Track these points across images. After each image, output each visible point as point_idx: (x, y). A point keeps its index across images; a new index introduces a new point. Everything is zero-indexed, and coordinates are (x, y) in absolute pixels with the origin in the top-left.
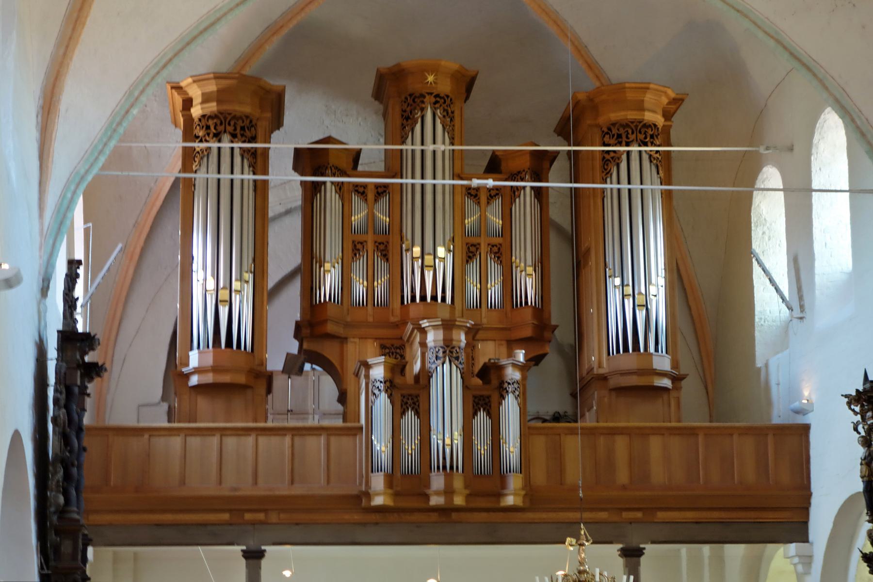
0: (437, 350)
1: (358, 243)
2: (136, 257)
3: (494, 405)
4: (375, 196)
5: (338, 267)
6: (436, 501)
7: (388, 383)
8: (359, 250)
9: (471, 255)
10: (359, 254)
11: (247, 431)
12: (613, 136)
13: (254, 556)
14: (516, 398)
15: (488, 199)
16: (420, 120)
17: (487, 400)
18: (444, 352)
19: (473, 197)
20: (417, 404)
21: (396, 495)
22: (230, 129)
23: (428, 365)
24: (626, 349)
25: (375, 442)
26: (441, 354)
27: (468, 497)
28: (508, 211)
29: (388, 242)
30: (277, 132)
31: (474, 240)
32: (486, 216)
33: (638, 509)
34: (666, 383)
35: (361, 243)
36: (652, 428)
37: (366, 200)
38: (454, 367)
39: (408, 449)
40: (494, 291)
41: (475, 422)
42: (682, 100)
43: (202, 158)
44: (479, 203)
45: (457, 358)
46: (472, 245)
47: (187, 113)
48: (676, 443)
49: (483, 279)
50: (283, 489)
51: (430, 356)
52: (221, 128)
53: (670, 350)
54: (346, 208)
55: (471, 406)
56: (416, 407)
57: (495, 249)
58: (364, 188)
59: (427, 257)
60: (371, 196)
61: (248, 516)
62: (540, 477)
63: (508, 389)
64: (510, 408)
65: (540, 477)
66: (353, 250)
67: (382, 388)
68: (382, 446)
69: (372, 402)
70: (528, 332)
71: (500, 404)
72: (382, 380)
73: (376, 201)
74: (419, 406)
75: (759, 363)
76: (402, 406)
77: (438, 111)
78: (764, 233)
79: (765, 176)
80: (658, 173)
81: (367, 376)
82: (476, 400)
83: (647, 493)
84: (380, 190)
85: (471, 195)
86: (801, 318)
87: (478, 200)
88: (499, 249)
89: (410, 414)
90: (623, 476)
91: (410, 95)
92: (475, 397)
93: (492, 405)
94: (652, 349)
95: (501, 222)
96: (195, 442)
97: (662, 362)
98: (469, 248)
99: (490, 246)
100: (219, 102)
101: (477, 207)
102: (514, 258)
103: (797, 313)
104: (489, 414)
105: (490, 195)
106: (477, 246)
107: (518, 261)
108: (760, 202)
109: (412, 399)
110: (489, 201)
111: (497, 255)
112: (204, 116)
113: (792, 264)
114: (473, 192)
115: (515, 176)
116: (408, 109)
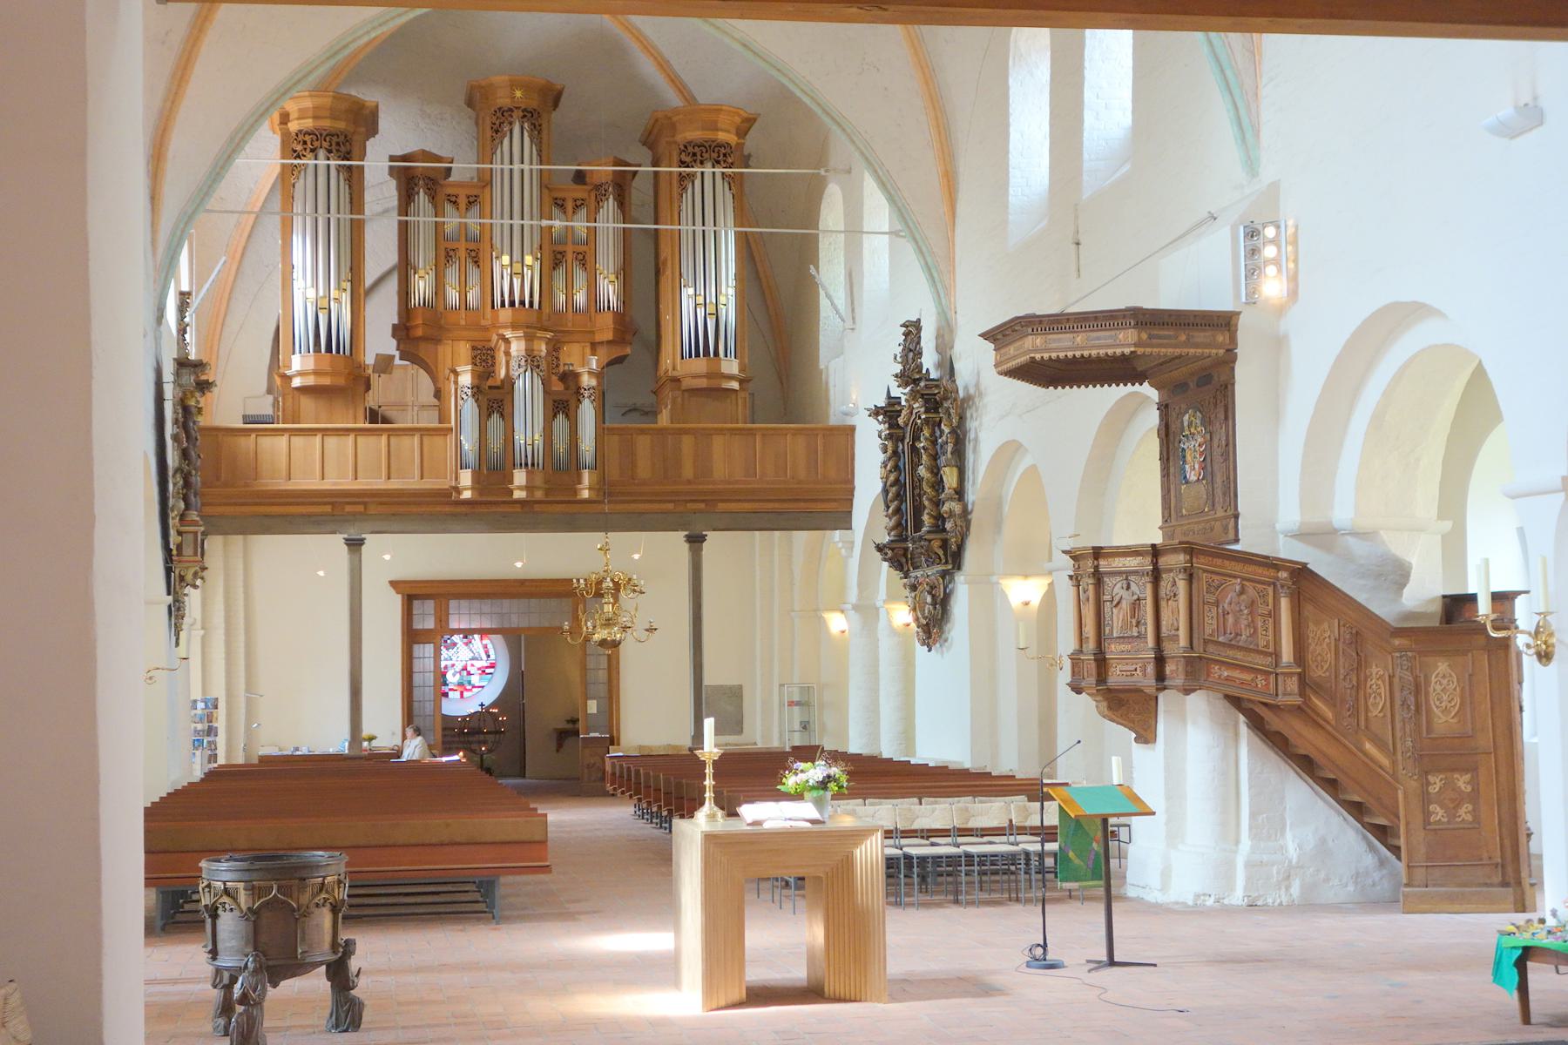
2: (238, 256)
3: (572, 407)
5: (432, 274)
6: (519, 494)
9: (558, 262)
11: (347, 431)
12: (689, 154)
13: (355, 545)
18: (526, 361)
22: (325, 144)
23: (511, 372)
24: (698, 355)
25: (464, 442)
26: (523, 363)
27: (548, 492)
30: (372, 139)
31: (560, 248)
33: (703, 501)
34: (735, 385)
36: (716, 429)
38: (535, 375)
40: (580, 298)
41: (554, 424)
42: (755, 120)
43: (299, 172)
45: (538, 367)
47: (284, 126)
50: (380, 484)
51: (514, 364)
52: (317, 144)
53: (738, 355)
57: (581, 257)
59: (514, 265)
60: (463, 205)
61: (348, 508)
62: (613, 472)
64: (587, 412)
65: (613, 472)
67: (469, 394)
68: (469, 443)
70: (609, 336)
71: (577, 407)
72: (470, 386)
75: (822, 366)
76: (488, 409)
77: (526, 125)
78: (830, 244)
80: (730, 189)
81: (456, 383)
82: (556, 404)
83: (711, 487)
84: (471, 199)
85: (558, 205)
86: (853, 329)
88: (584, 257)
89: (495, 416)
90: (688, 471)
91: (500, 109)
96: (298, 441)
97: (731, 366)
98: (555, 255)
100: (315, 117)
102: (598, 265)
103: (849, 324)
104: (567, 416)
105: (576, 206)
112: (300, 131)
113: (847, 277)
114: (560, 202)
116: (497, 123)
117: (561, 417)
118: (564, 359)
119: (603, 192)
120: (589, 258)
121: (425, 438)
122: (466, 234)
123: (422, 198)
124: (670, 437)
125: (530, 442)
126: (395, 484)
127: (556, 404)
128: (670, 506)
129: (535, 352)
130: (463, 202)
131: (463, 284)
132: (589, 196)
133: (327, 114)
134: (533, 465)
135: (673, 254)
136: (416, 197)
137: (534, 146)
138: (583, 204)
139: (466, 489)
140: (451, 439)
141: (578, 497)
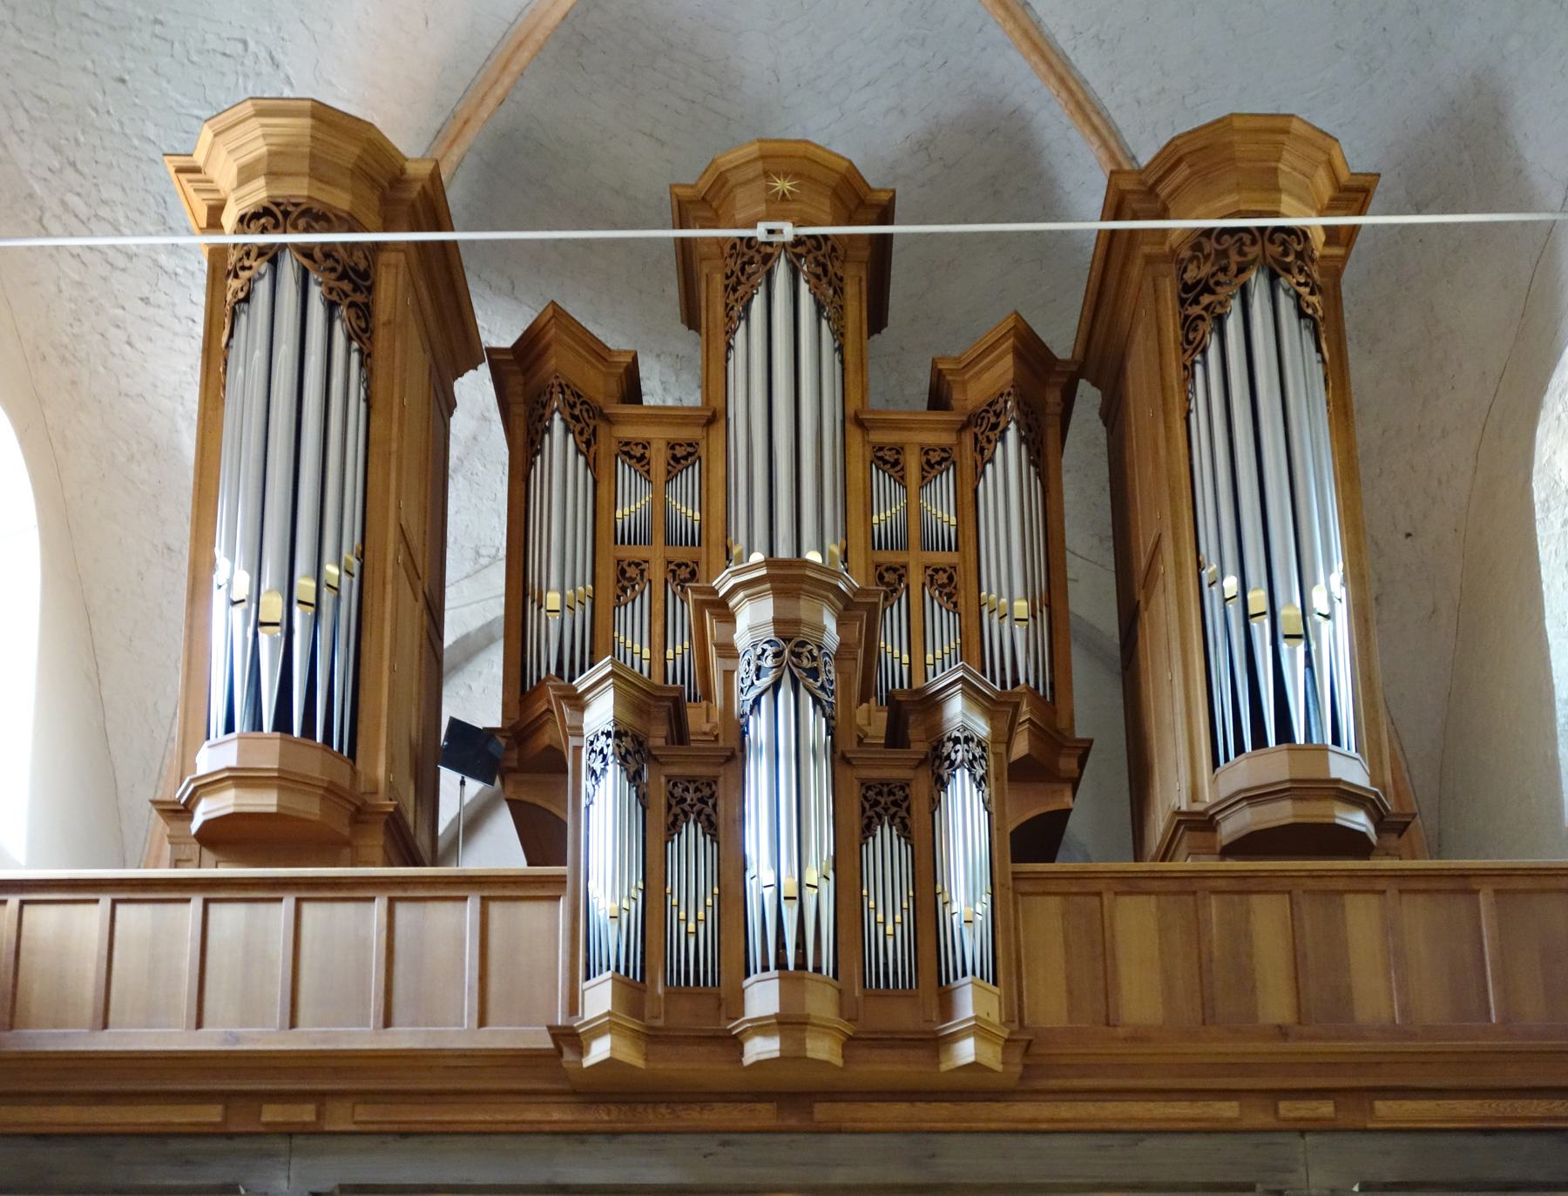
3: (919, 805)
4: (669, 464)
8: (631, 579)
14: (979, 786)
15: (923, 469)
19: (889, 466)
20: (711, 802)
21: (651, 1038)
27: (850, 1043)
28: (969, 496)
30: (471, 372)
32: (920, 508)
37: (648, 472)
39: (687, 920)
44: (902, 477)
48: (1417, 915)
56: (708, 810)
58: (644, 447)
67: (609, 751)
69: (588, 795)
71: (935, 804)
73: (670, 476)
74: (715, 806)
76: (669, 807)
84: (680, 452)
85: (886, 462)
87: (900, 474)
89: (691, 832)
90: (1276, 1006)
92: (866, 785)
93: (914, 809)
94: (1329, 741)
101: (900, 491)
104: (905, 832)
105: (928, 462)
108: (1554, 453)
109: (697, 790)
110: (926, 474)
114: (889, 456)
115: (984, 414)
117: (885, 837)
120: (963, 579)
121: (495, 909)
122: (666, 524)
123: (558, 441)
124: (1214, 901)
125: (789, 886)
127: (871, 794)
128: (1228, 1110)
132: (960, 443)
134: (801, 965)
135: (1175, 514)
136: (547, 437)
138: (944, 460)
139: (596, 1033)
140: (563, 906)
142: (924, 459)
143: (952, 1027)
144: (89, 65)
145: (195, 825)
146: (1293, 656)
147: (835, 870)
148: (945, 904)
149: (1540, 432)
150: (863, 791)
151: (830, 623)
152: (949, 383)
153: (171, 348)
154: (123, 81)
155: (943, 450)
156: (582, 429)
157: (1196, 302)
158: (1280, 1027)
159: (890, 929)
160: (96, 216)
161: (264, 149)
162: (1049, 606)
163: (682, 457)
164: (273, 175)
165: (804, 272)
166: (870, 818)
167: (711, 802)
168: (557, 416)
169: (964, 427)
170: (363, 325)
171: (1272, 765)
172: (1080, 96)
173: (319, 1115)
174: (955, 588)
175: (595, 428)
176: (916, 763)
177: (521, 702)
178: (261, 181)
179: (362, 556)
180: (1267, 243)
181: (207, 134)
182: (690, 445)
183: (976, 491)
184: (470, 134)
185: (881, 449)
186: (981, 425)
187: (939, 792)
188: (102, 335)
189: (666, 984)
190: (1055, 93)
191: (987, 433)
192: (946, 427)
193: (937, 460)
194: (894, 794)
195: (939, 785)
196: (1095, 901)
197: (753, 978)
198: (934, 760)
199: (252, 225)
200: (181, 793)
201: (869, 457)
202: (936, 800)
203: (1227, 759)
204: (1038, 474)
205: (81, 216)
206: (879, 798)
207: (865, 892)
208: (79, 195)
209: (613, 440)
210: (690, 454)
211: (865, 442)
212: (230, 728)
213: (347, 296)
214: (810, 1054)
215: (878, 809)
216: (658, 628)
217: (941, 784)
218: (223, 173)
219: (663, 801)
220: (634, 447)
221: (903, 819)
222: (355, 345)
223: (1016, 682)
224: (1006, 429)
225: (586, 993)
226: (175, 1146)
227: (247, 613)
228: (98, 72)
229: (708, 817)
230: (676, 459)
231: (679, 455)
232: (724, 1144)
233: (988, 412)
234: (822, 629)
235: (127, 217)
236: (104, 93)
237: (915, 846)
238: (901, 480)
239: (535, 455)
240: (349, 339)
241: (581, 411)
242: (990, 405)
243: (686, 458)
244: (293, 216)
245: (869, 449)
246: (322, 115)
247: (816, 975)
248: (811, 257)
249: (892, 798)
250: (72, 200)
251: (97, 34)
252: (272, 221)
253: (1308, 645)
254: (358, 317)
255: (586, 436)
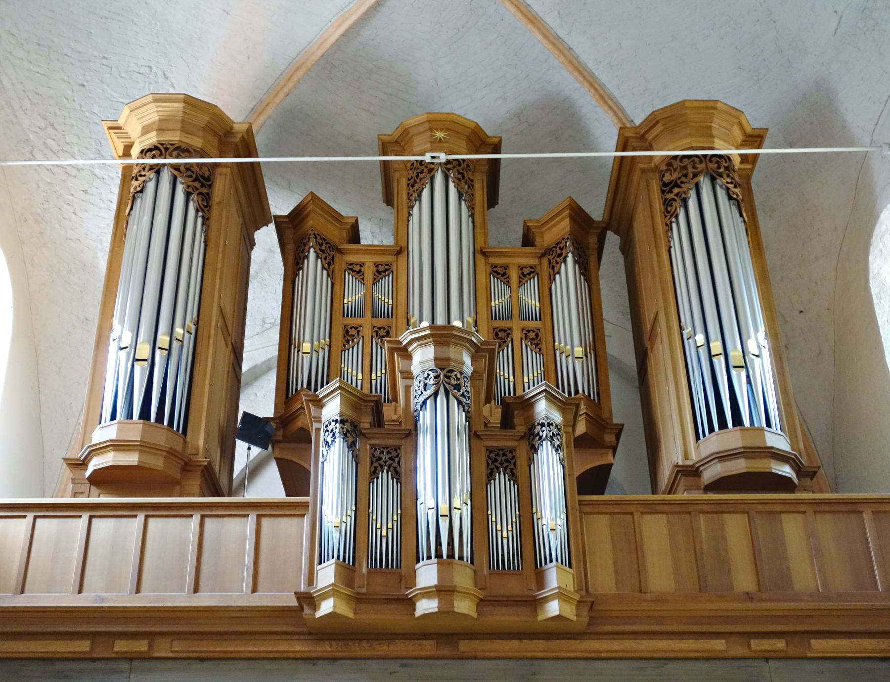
0: (426, 375)
1: (351, 328)
3: (521, 461)
4: (375, 275)
7: (349, 424)
10: (353, 340)
14: (557, 450)
15: (520, 277)
16: (428, 186)
17: (510, 456)
18: (436, 377)
19: (500, 276)
20: (396, 460)
21: (359, 600)
26: (431, 381)
27: (481, 603)
29: (390, 327)
30: (265, 227)
32: (519, 298)
35: (356, 328)
37: (363, 279)
38: (454, 403)
39: (381, 528)
43: (134, 199)
46: (500, 331)
49: (517, 368)
54: (337, 288)
55: (484, 465)
56: (395, 464)
58: (361, 266)
63: (541, 434)
66: (345, 337)
69: (323, 456)
71: (531, 461)
73: (375, 281)
74: (399, 462)
76: (372, 463)
79: (884, 227)
80: (741, 215)
84: (381, 268)
87: (507, 280)
88: (537, 335)
89: (385, 477)
92: (490, 450)
93: (518, 463)
95: (538, 304)
97: (778, 441)
99: (525, 332)
101: (507, 289)
104: (513, 477)
105: (523, 274)
106: (508, 332)
107: (562, 345)
109: (388, 453)
111: (535, 342)
114: (500, 270)
115: (554, 249)
117: (501, 479)
118: (504, 373)
119: (559, 252)
122: (373, 306)
123: (312, 263)
125: (444, 509)
126: (205, 599)
127: (492, 455)
129: (452, 363)
130: (369, 272)
131: (367, 369)
132: (540, 264)
133: (179, 126)
134: (451, 555)
135: (665, 300)
136: (306, 261)
137: (463, 202)
139: (324, 596)
140: (306, 520)
141: (540, 618)
142: (520, 272)
143: (544, 593)
144: (66, 78)
145: (88, 473)
146: (739, 378)
147: (471, 499)
148: (538, 519)
149: (871, 257)
150: (488, 453)
151: (467, 359)
152: (533, 233)
153: (98, 216)
154: (83, 85)
155: (531, 267)
156: (326, 257)
157: (671, 191)
158: (748, 594)
159: (505, 534)
160: (62, 150)
161: (157, 118)
162: (595, 350)
163: (382, 271)
164: (160, 130)
165: (452, 177)
166: (492, 469)
167: (396, 460)
168: (312, 250)
169: (543, 255)
170: (205, 204)
171: (731, 439)
172: (601, 92)
173: (150, 646)
174: (540, 340)
175: (333, 256)
176: (518, 438)
177: (286, 403)
178: (154, 133)
179: (197, 323)
180: (708, 162)
181: (126, 110)
182: (387, 265)
183: (550, 289)
184: (269, 111)
185: (496, 267)
186: (552, 255)
187: (533, 454)
188: (60, 209)
189: (368, 567)
190: (588, 90)
191: (556, 259)
192: (533, 255)
193: (525, 275)
194: (506, 455)
195: (533, 450)
196: (629, 517)
197: (421, 563)
198: (530, 436)
199: (147, 155)
200: (80, 454)
201: (489, 270)
202: (532, 458)
203: (704, 435)
204: (585, 280)
205: (54, 150)
206: (497, 458)
207: (489, 512)
208: (54, 140)
209: (343, 262)
210: (387, 270)
211: (486, 263)
212: (113, 417)
213: (197, 189)
214: (456, 610)
215: (497, 464)
216: (367, 362)
217: (534, 449)
218: (134, 129)
219: (368, 459)
220: (355, 266)
221: (512, 470)
222: (200, 214)
223: (577, 392)
224: (567, 256)
225: (319, 572)
226: (59, 666)
227: (128, 354)
228: (70, 81)
229: (395, 468)
230: (379, 272)
231: (381, 270)
232: (405, 666)
233: (556, 247)
234: (463, 363)
235: (79, 150)
236: (73, 91)
237: (520, 486)
238: (508, 283)
239: (299, 270)
240: (197, 211)
241: (326, 247)
242: (557, 244)
243: (384, 272)
244: (171, 150)
245: (488, 267)
246: (190, 102)
247: (460, 562)
248: (455, 170)
249: (505, 458)
250: (50, 142)
251: (72, 64)
252: (159, 152)
253: (748, 372)
254: (203, 200)
255: (328, 260)
